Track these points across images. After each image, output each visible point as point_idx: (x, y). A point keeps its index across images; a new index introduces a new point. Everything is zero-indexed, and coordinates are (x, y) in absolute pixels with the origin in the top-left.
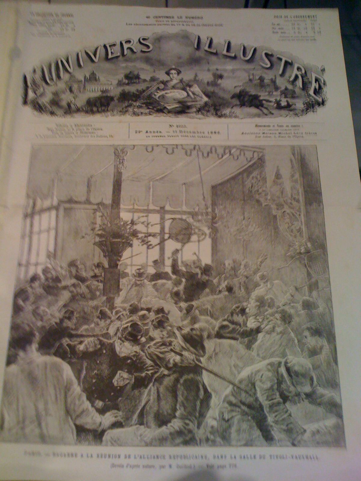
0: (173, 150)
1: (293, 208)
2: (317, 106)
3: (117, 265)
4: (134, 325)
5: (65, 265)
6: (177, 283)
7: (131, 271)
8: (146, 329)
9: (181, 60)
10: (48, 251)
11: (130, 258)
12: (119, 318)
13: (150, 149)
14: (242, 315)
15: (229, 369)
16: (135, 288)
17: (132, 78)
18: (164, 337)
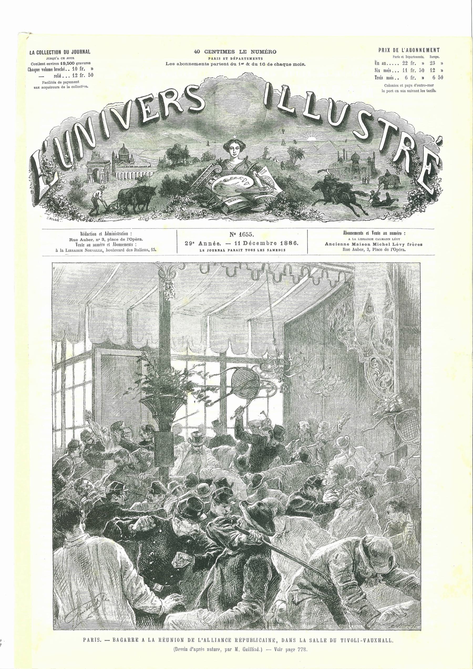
0: (235, 271)
1: (384, 354)
2: (426, 203)
3: (170, 427)
4: (193, 500)
5: (107, 428)
6: (242, 449)
7: (186, 434)
8: (206, 504)
9: (244, 126)
10: (85, 411)
11: (184, 418)
12: (175, 493)
13: (205, 269)
14: (318, 489)
15: (301, 548)
16: (192, 456)
17: (177, 156)
18: (227, 513)
